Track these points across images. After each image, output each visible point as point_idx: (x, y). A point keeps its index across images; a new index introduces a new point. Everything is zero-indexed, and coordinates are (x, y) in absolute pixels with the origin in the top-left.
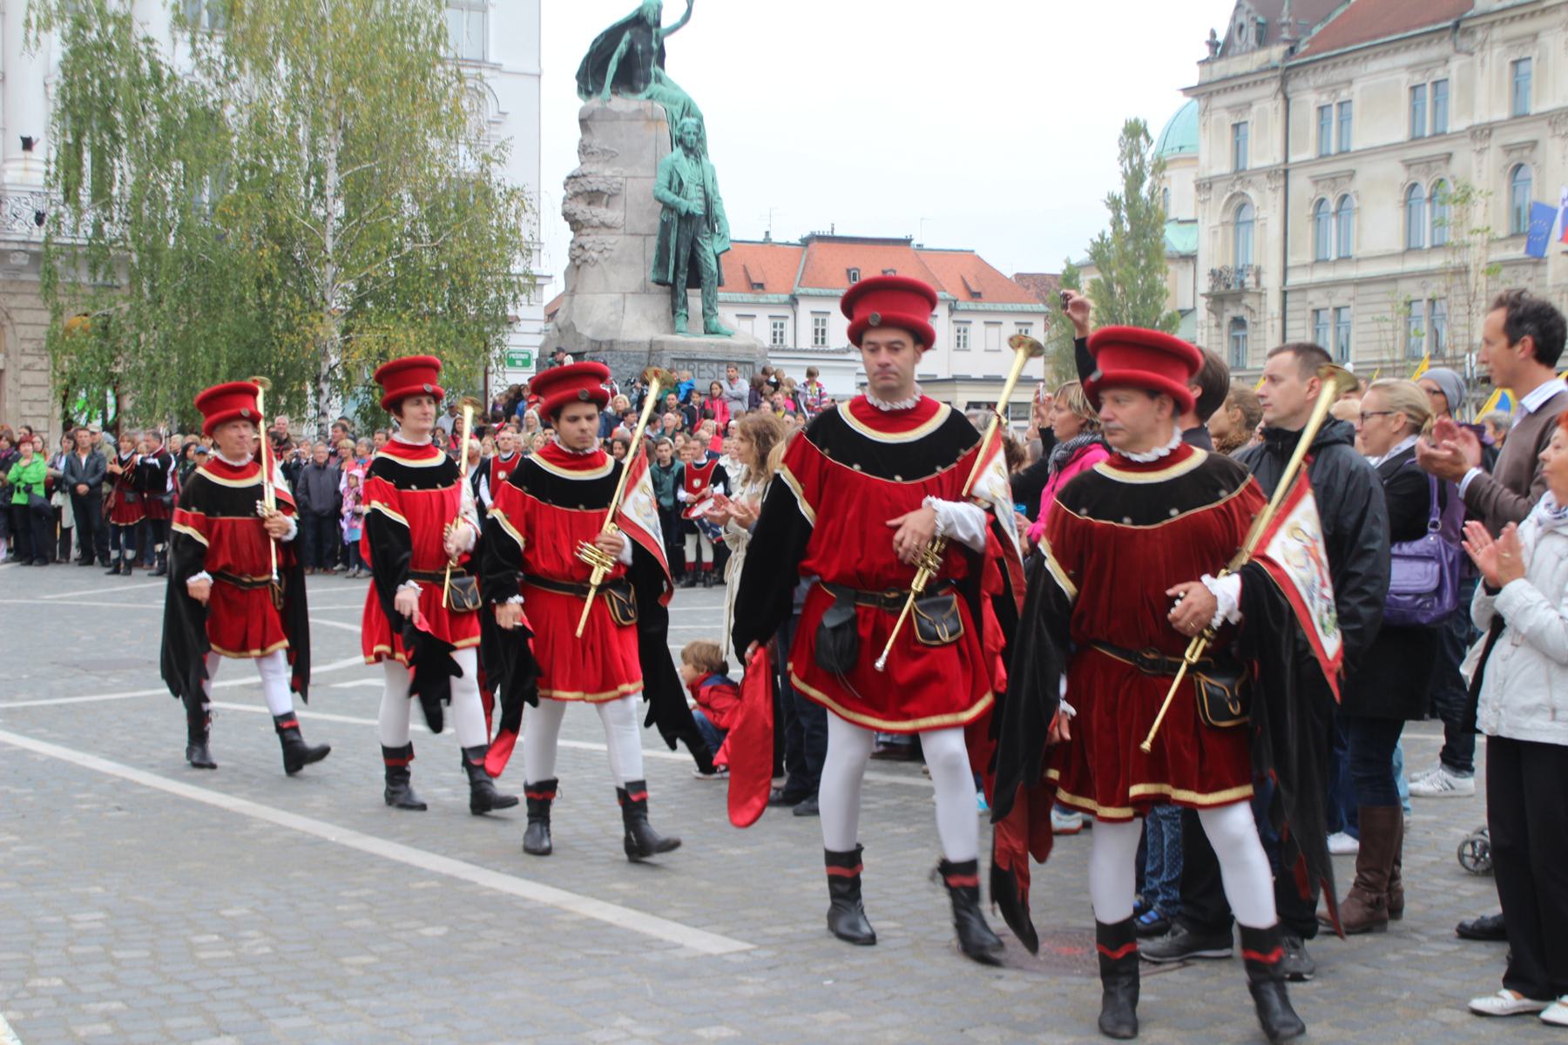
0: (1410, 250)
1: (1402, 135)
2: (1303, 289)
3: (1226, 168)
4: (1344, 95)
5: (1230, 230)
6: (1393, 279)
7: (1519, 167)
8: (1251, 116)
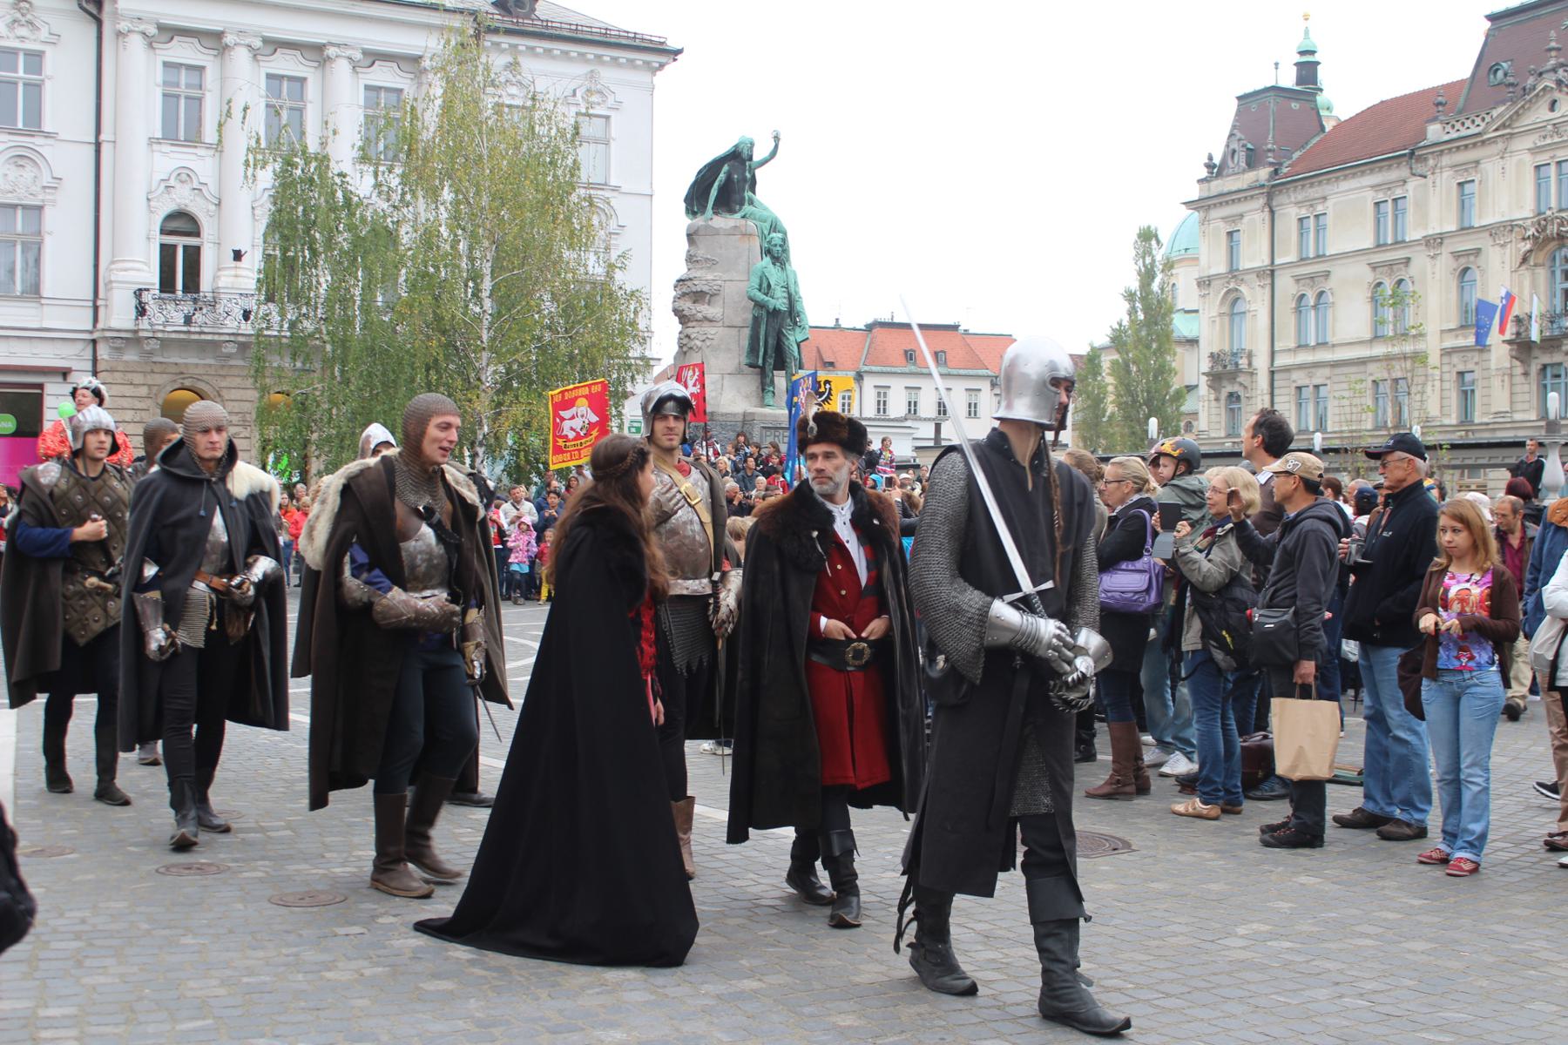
0: (1376, 338)
1: (1368, 242)
2: (1287, 369)
3: (1222, 268)
4: (1320, 209)
5: (1226, 319)
6: (1362, 362)
7: (1466, 270)
8: (1242, 226)
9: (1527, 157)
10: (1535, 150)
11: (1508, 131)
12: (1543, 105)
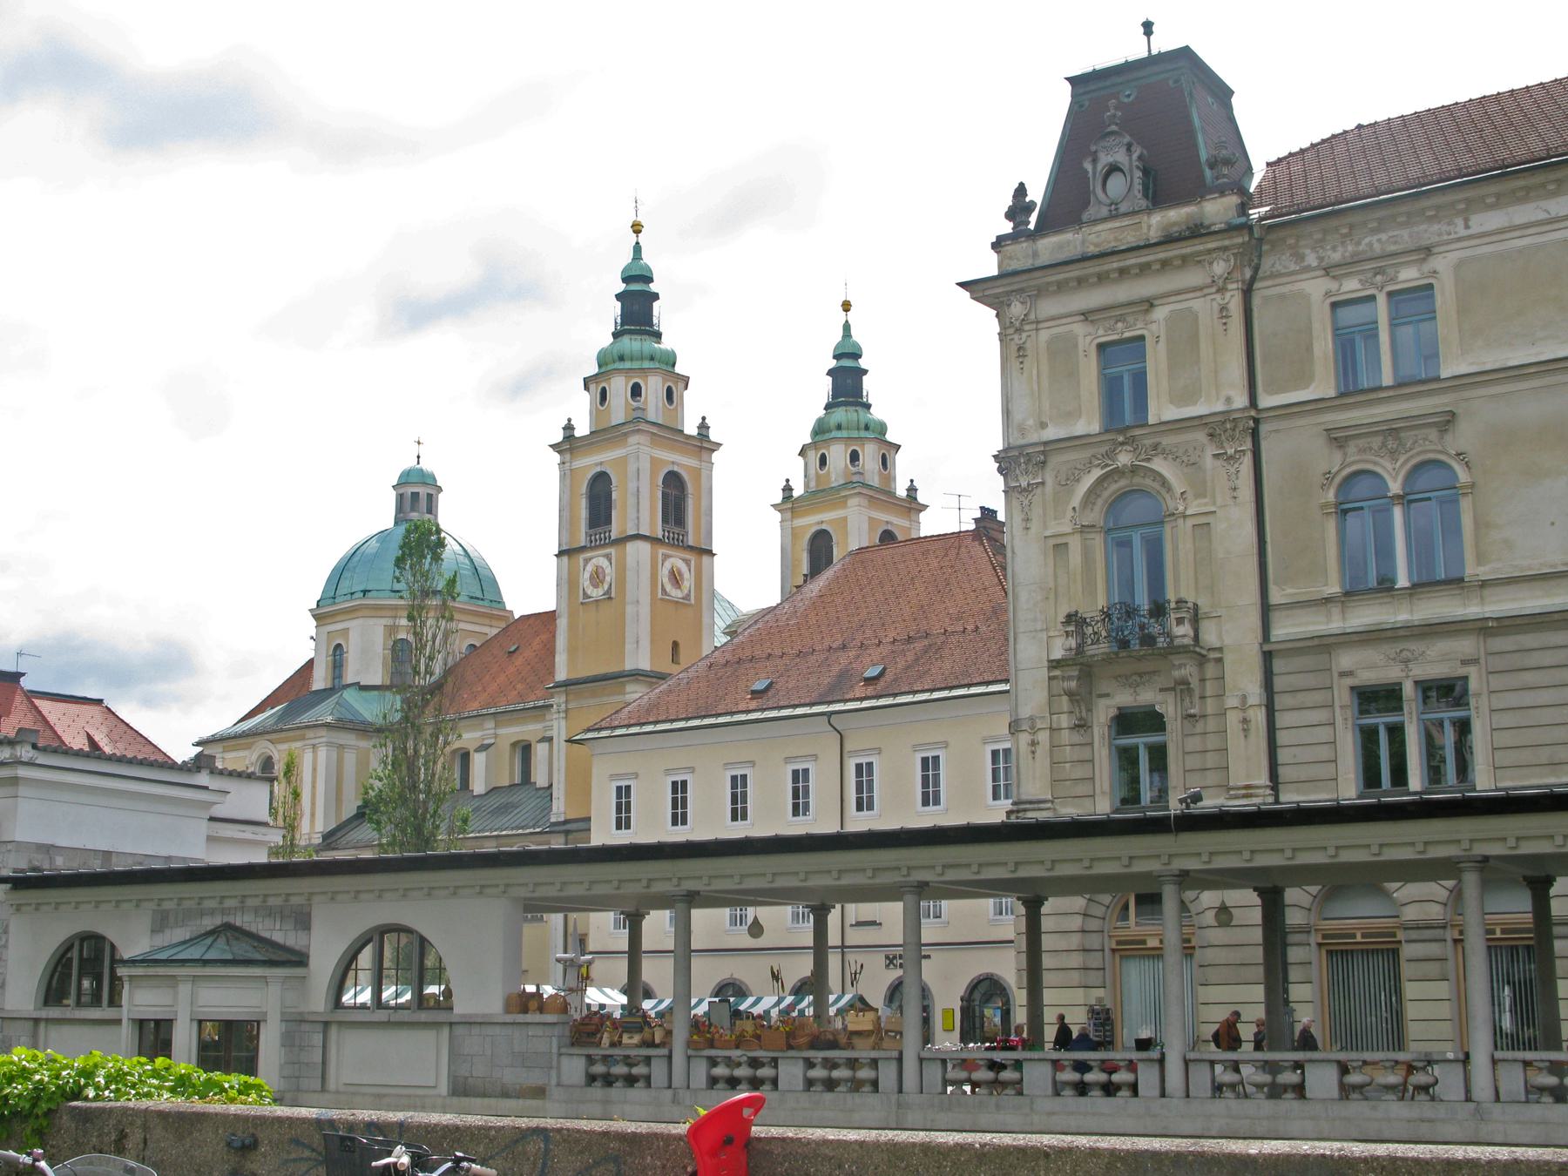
2: (1325, 645)
5: (1098, 541)
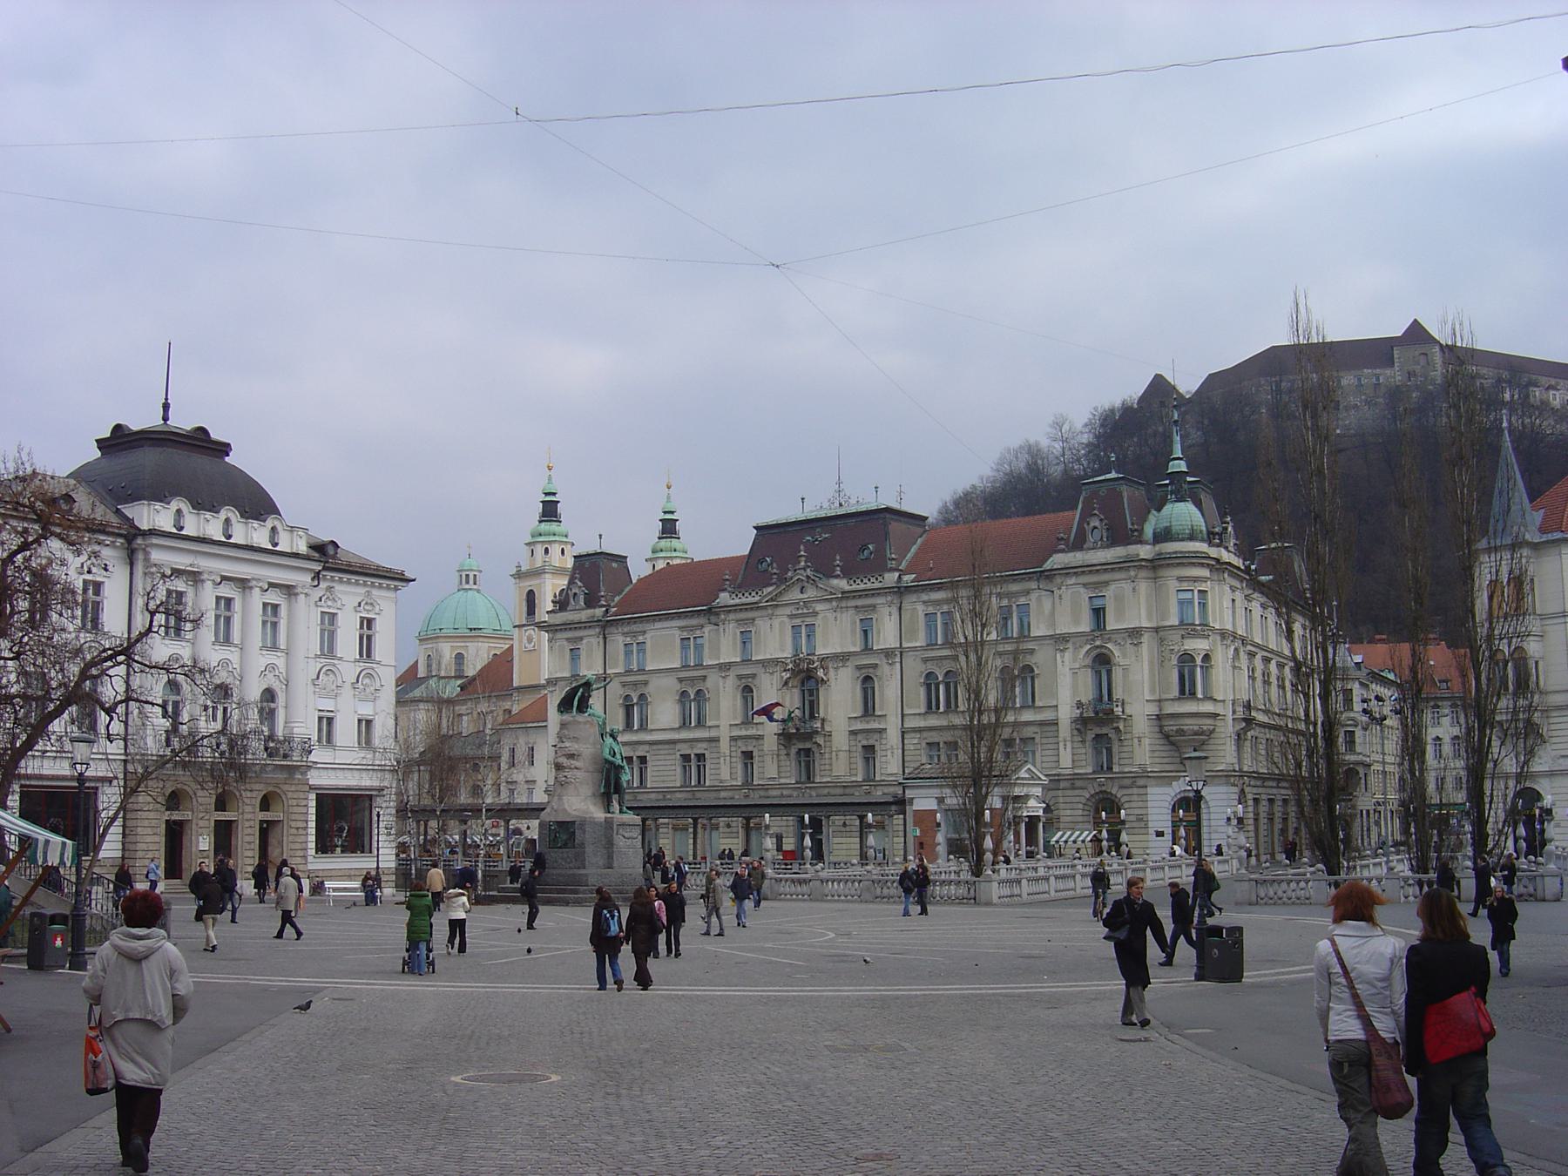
0: (684, 724)
4: (641, 639)
8: (583, 645)
9: (786, 620)
10: (791, 617)
11: (774, 604)
12: (797, 589)
